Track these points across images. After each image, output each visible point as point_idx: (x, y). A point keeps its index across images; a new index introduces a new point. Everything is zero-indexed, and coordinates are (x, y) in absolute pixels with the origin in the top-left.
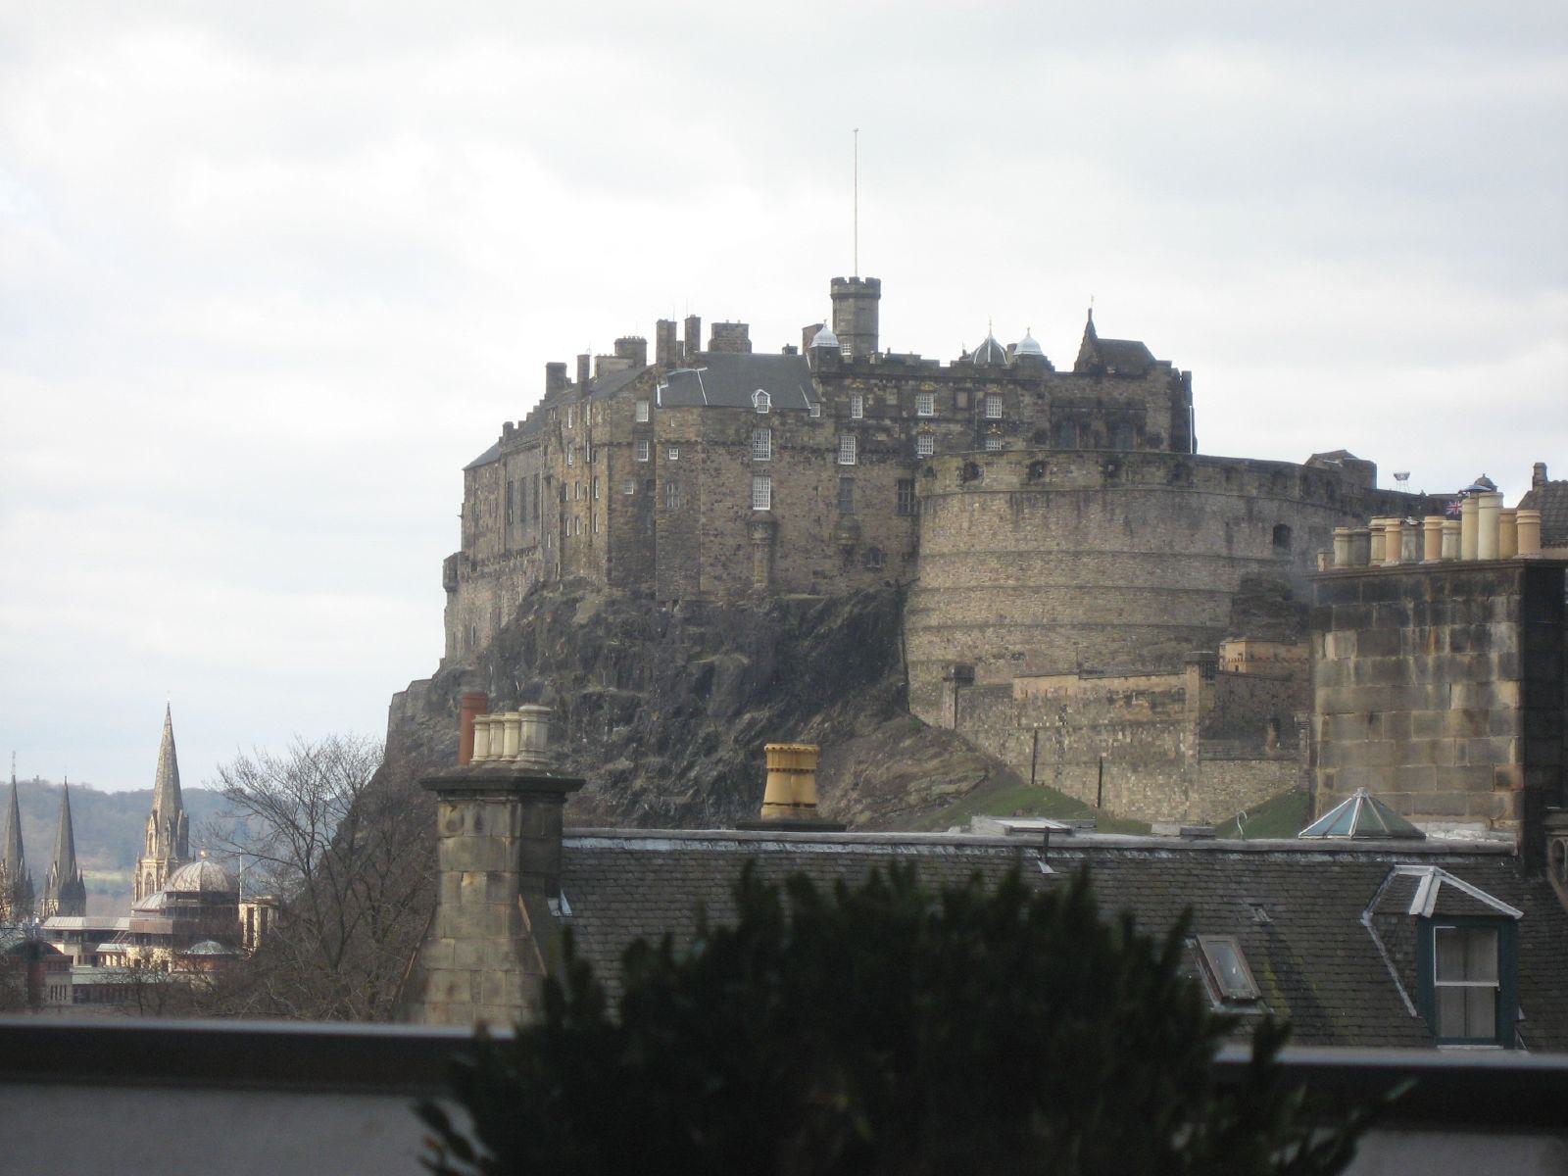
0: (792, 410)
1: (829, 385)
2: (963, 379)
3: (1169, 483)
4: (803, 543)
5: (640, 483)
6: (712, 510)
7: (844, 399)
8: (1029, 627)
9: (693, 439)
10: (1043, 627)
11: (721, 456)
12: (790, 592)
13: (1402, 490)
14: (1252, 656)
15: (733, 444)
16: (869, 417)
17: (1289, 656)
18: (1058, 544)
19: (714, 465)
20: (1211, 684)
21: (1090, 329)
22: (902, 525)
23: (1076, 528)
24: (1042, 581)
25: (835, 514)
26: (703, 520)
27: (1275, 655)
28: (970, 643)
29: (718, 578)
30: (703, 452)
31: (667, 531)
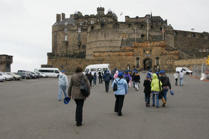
0: (70, 24)
2: (98, 17)
3: (114, 27)
4: (72, 45)
7: (79, 22)
9: (56, 30)
11: (60, 33)
12: (70, 53)
13: (192, 31)
14: (94, 55)
16: (83, 25)
17: (103, 55)
20: (51, 60)
21: (151, 15)
25: (77, 40)
26: (58, 43)
27: (100, 55)
29: (60, 51)
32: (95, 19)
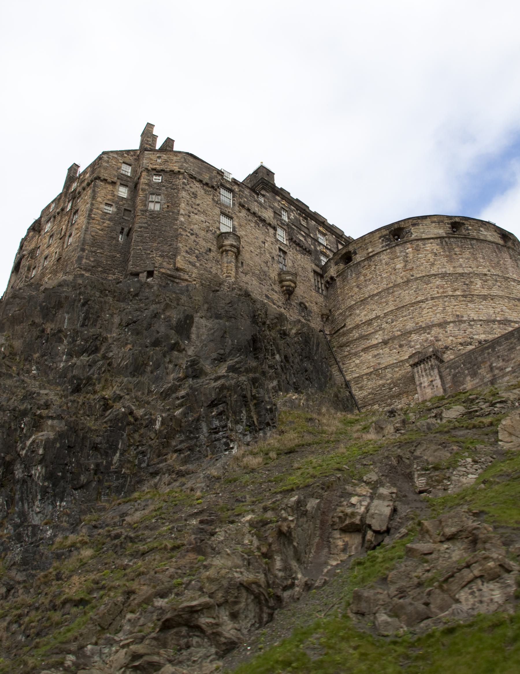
1: (268, 192)
5: (118, 209)
6: (189, 216)
8: (488, 322)
9: (176, 169)
10: (499, 321)
15: (207, 184)
18: (489, 271)
19: (192, 190)
22: (321, 299)
23: (498, 263)
24: (485, 292)
25: (277, 267)
28: (432, 338)
30: (185, 178)
31: (146, 223)
32: (333, 238)
